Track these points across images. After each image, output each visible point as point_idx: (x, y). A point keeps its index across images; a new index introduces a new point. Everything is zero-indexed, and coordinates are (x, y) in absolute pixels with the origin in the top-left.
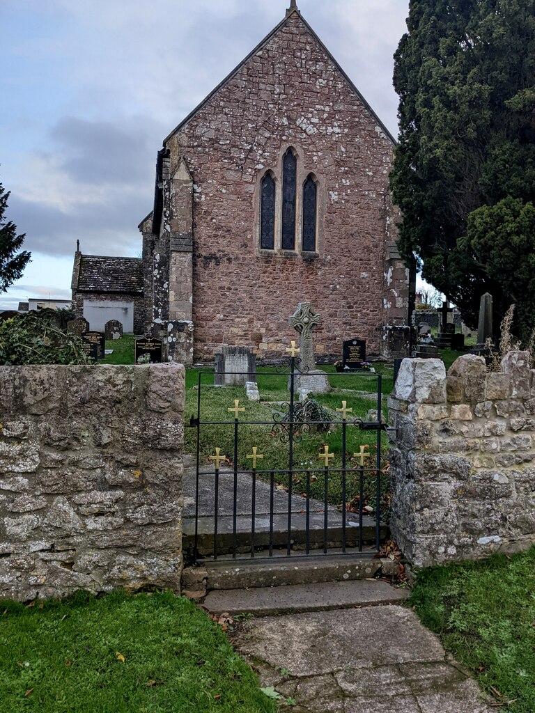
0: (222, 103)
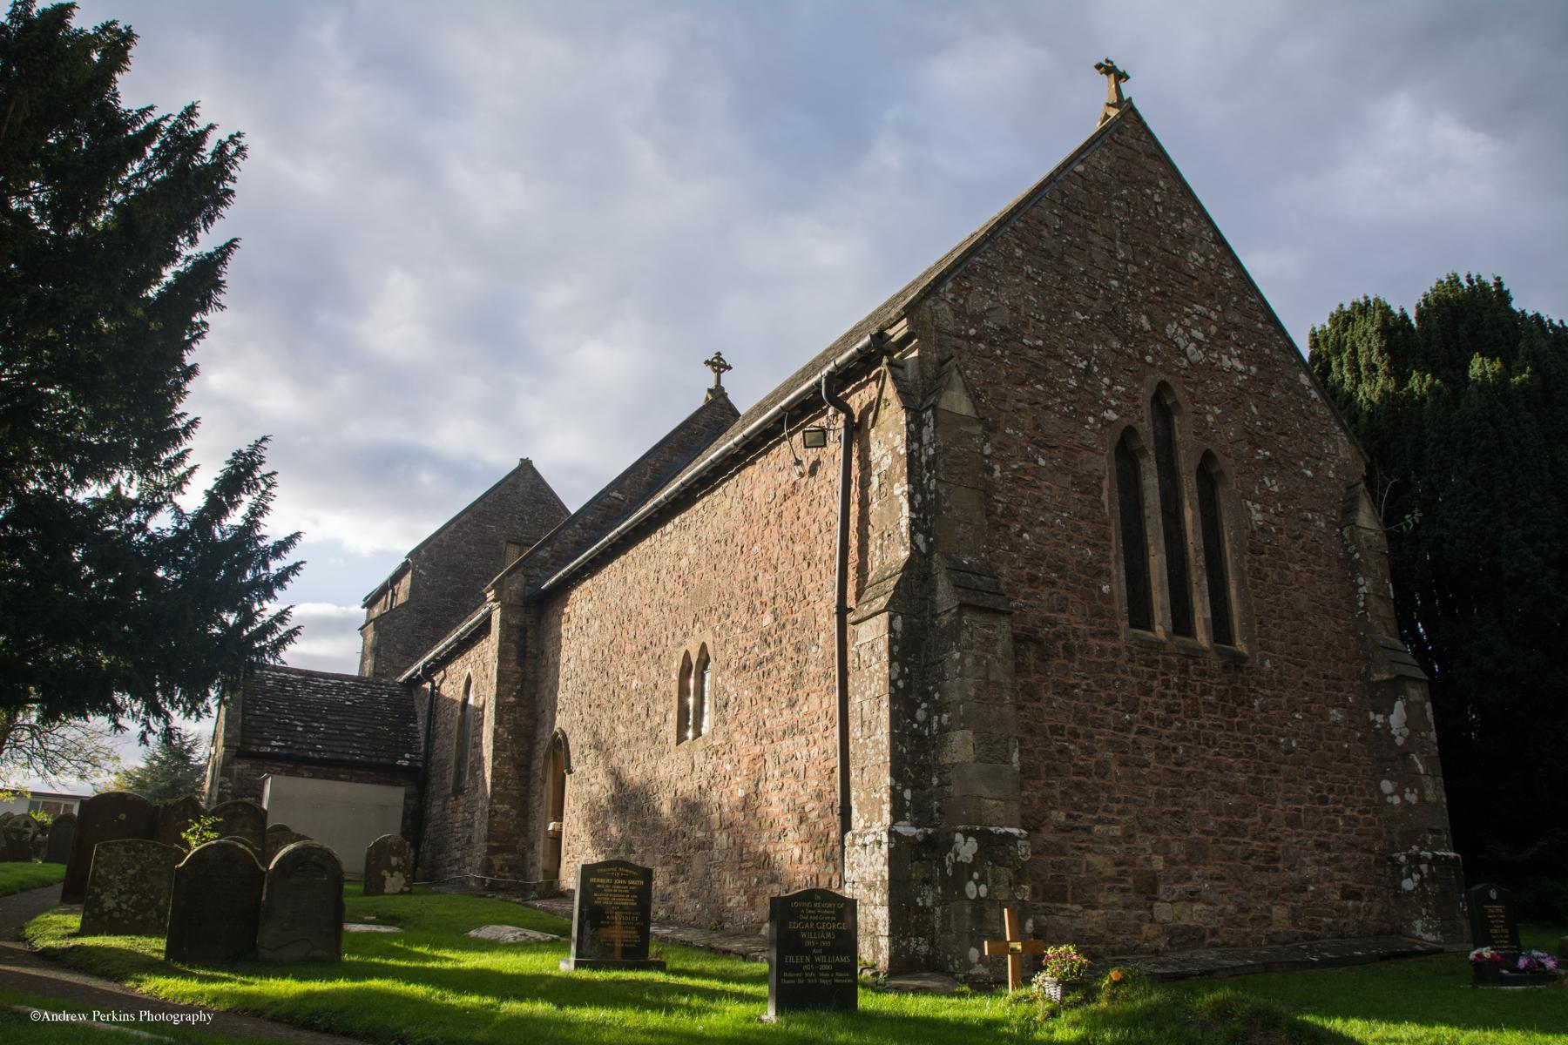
0: (1019, 253)
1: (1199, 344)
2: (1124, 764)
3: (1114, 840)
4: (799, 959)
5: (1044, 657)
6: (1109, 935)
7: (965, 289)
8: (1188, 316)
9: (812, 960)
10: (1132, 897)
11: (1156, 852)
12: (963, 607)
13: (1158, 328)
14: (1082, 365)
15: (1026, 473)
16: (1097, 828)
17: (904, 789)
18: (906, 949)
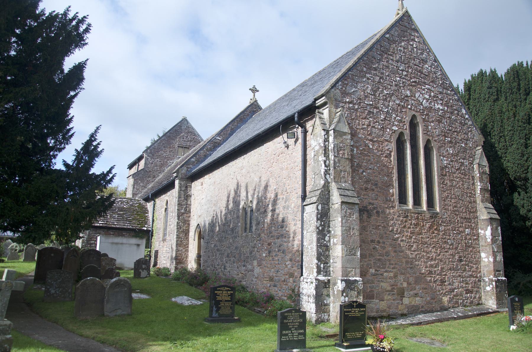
0: (365, 69)
1: (427, 100)
2: (395, 252)
3: (391, 278)
4: (287, 332)
5: (369, 216)
6: (388, 309)
7: (345, 84)
8: (424, 90)
9: (292, 332)
10: (395, 297)
11: (404, 281)
12: (343, 203)
13: (413, 95)
14: (386, 110)
15: (365, 151)
16: (385, 274)
17: (321, 264)
18: (320, 318)
